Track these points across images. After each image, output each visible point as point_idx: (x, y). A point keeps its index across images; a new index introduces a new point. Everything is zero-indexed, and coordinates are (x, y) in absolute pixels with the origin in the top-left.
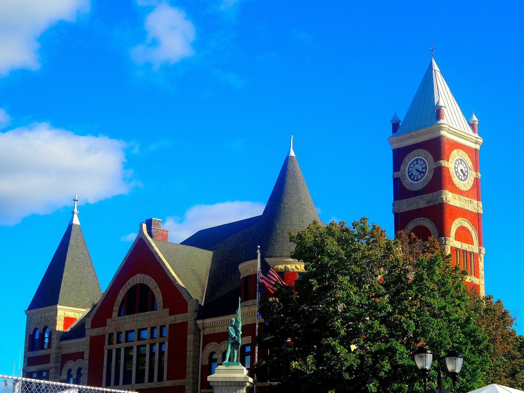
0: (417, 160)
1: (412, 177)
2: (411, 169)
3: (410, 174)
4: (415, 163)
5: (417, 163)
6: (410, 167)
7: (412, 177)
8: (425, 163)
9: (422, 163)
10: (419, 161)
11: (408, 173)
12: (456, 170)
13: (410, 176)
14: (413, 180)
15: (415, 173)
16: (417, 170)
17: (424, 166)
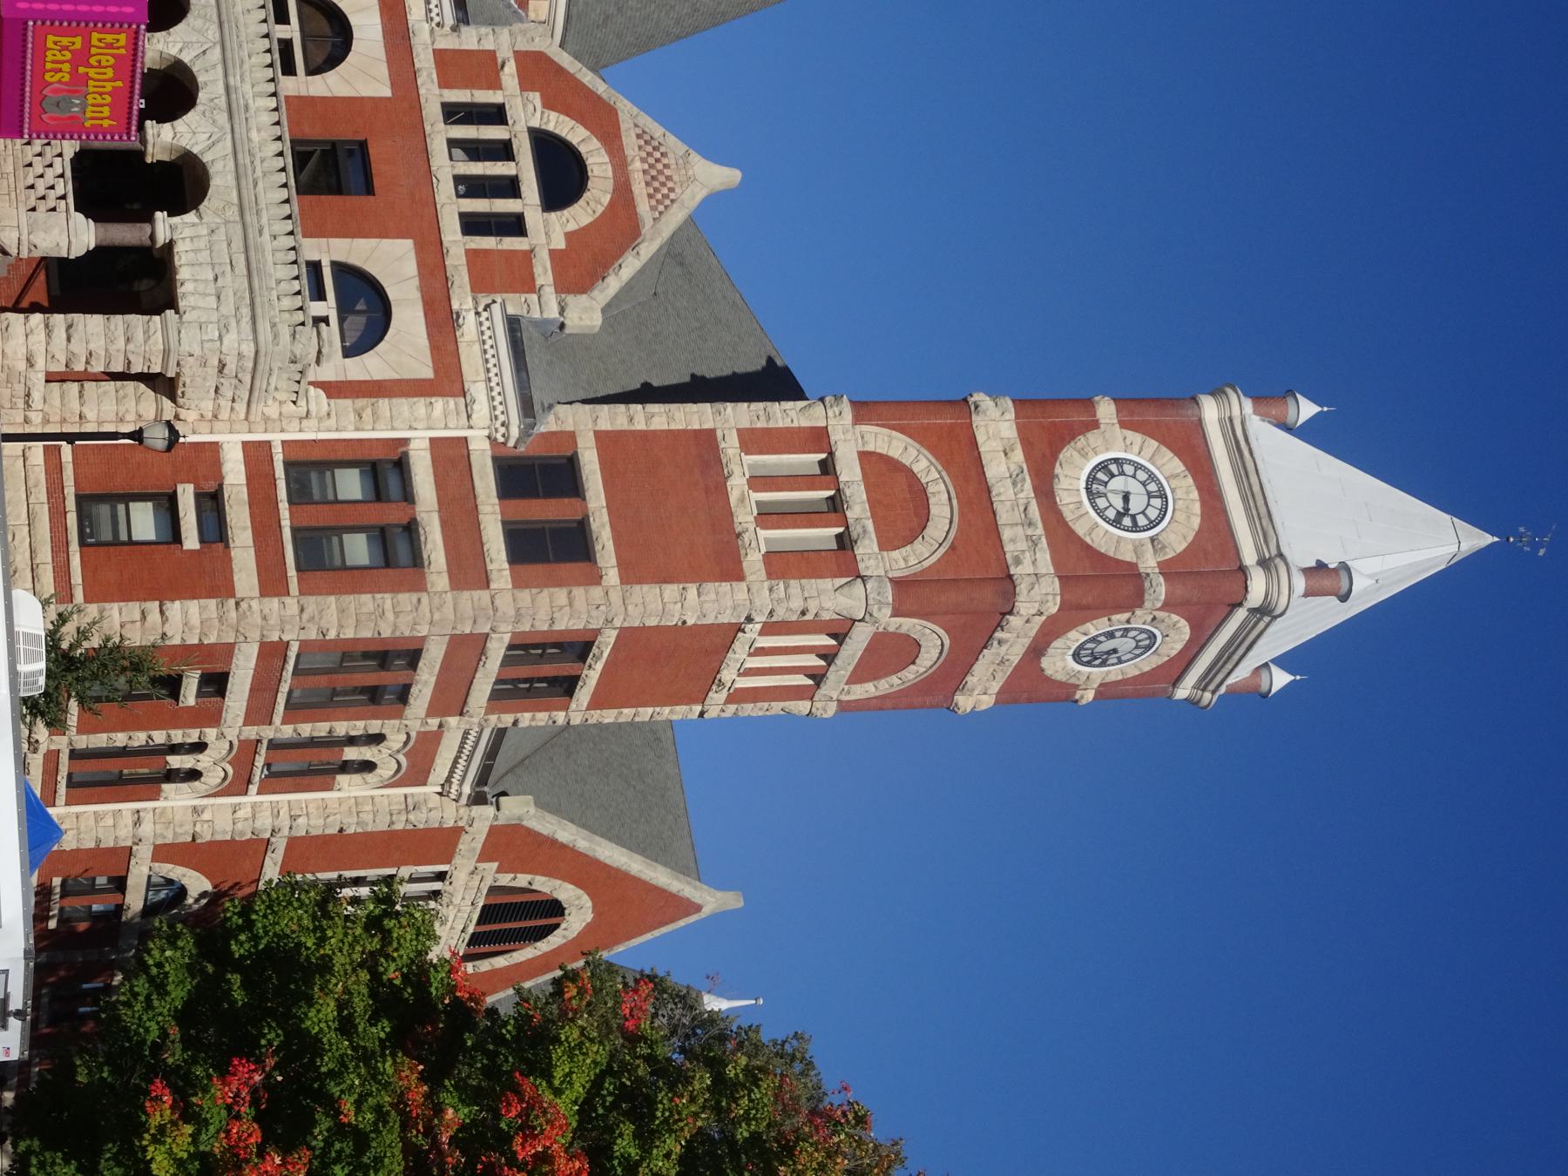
0: (1163, 496)
1: (1100, 475)
2: (1129, 469)
3: (1113, 468)
4: (1152, 487)
5: (1150, 495)
6: (1138, 467)
7: (1100, 475)
8: (1153, 524)
9: (1153, 513)
10: (1157, 502)
11: (1116, 461)
12: (1118, 634)
13: (1103, 466)
14: (1092, 479)
15: (1117, 483)
16: (1126, 498)
17: (1142, 521)
